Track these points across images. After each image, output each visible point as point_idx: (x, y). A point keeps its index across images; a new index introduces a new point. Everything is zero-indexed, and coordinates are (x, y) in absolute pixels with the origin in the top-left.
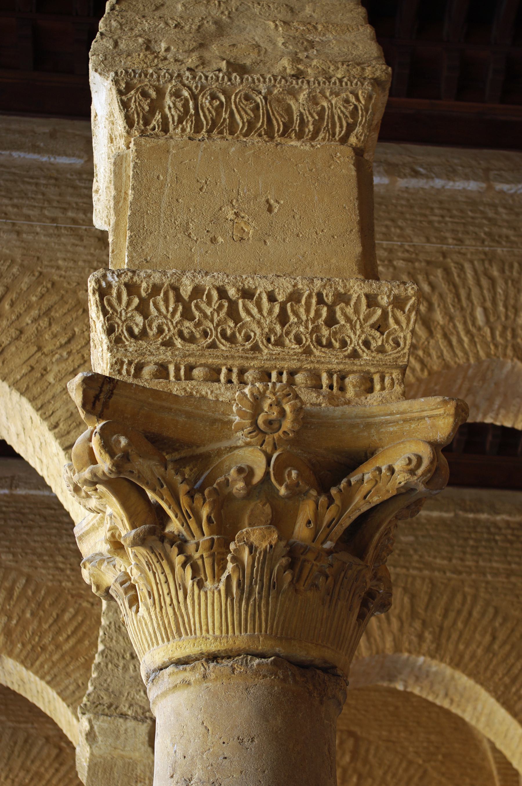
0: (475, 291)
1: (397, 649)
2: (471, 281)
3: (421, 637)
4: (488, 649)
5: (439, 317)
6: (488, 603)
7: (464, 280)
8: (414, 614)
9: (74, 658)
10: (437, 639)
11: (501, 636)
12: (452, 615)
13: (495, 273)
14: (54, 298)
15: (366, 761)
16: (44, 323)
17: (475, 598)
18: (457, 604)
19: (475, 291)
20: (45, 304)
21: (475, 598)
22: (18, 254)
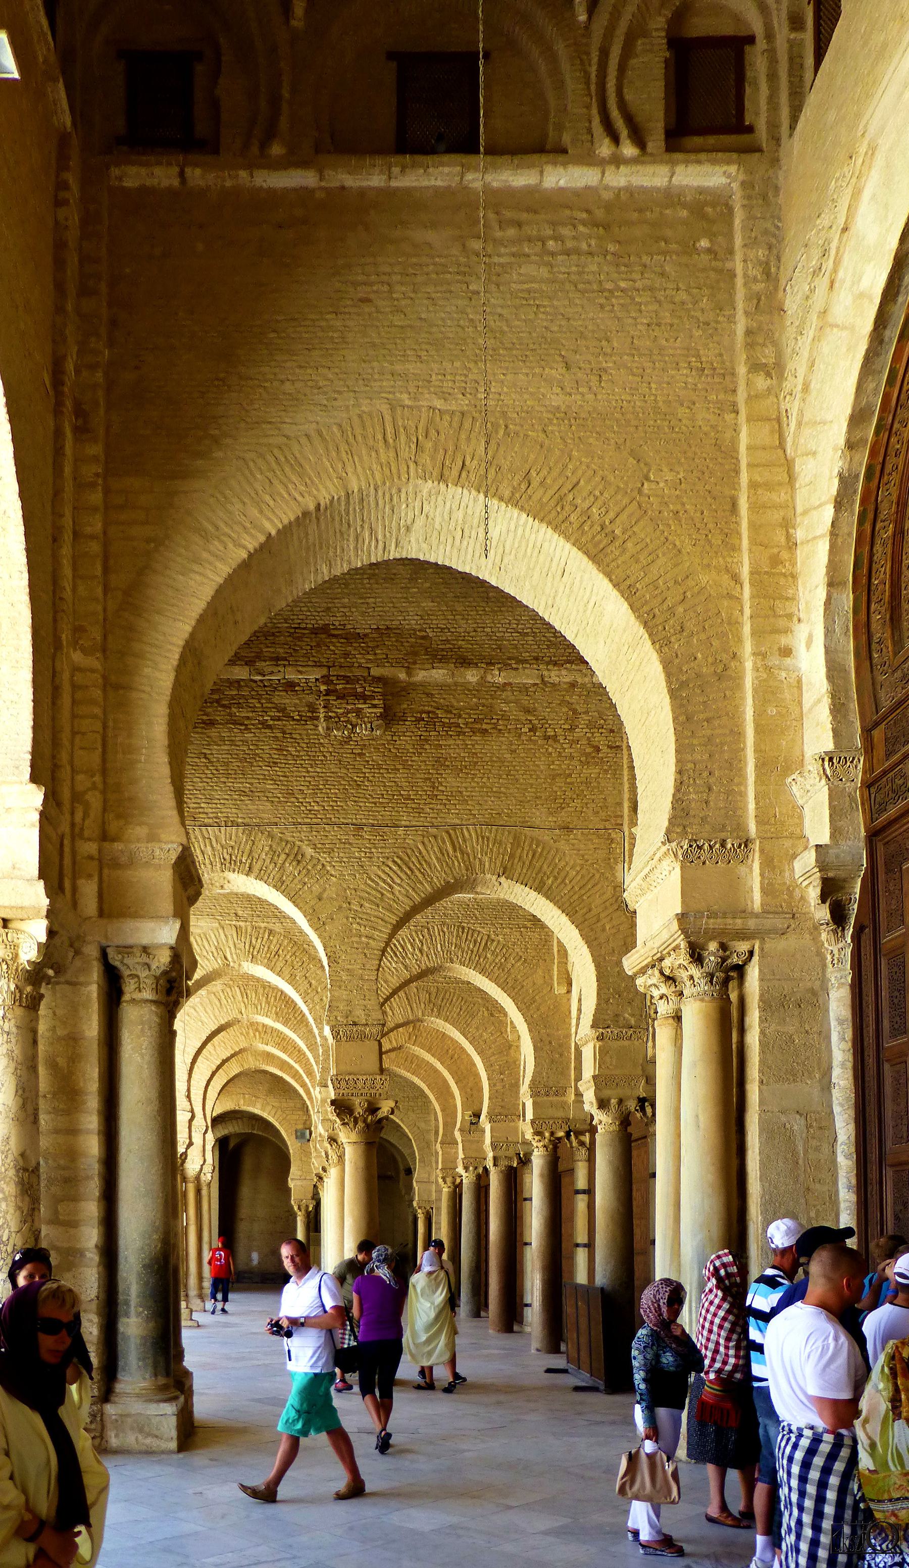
0: (438, 938)
1: (423, 1015)
2: (437, 934)
3: (432, 1010)
4: (458, 1014)
5: (425, 947)
6: (459, 995)
7: (434, 933)
8: (430, 1001)
9: (302, 1022)
10: (439, 1011)
11: (464, 1009)
12: (445, 1001)
13: (445, 929)
14: (295, 948)
15: (419, 1030)
16: (293, 958)
17: (454, 993)
18: (447, 996)
19: (438, 938)
20: (294, 950)
21: (454, 993)
22: (282, 931)
